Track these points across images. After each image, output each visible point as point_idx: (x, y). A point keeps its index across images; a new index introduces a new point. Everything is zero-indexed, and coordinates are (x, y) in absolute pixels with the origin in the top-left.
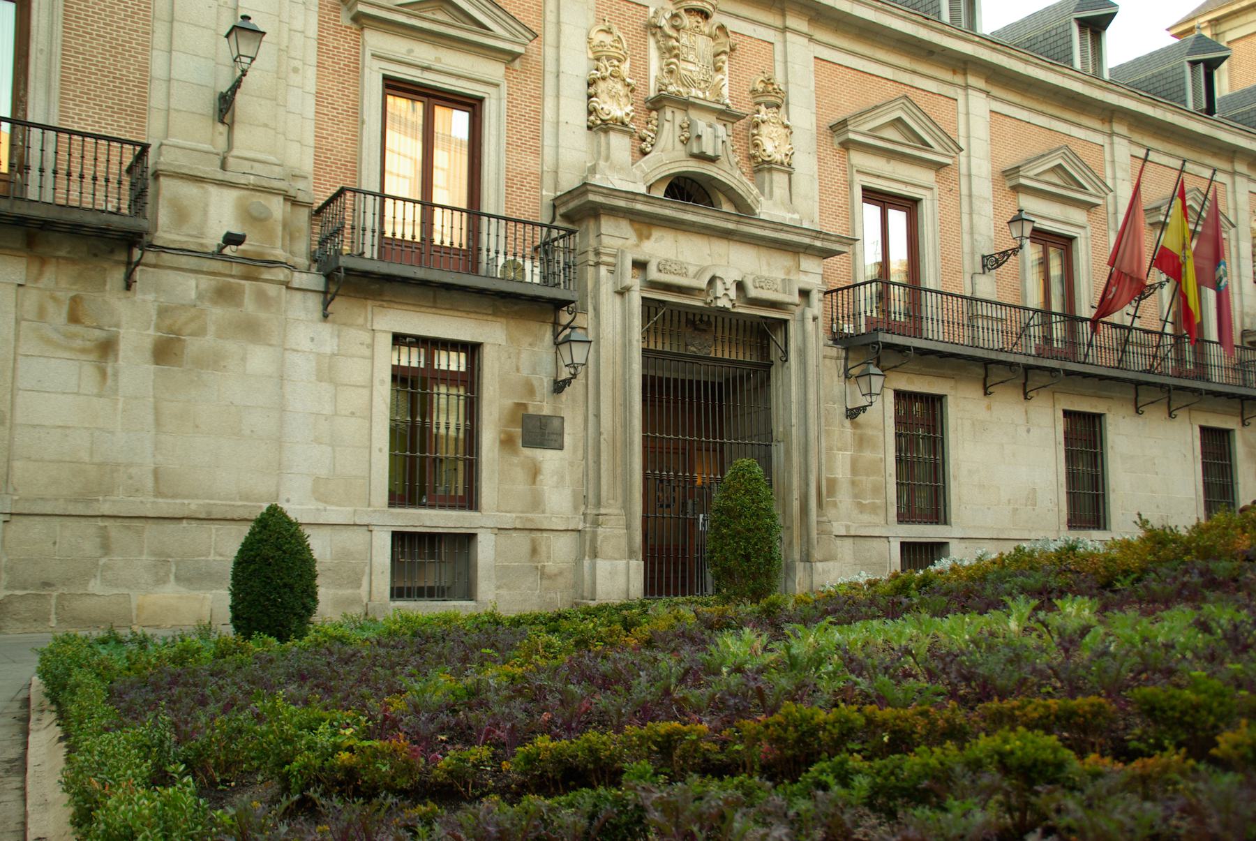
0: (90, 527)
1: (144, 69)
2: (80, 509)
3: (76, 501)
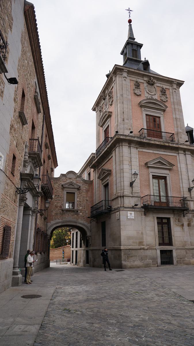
0: (184, 251)
1: (179, 186)
2: (183, 248)
3: (183, 247)
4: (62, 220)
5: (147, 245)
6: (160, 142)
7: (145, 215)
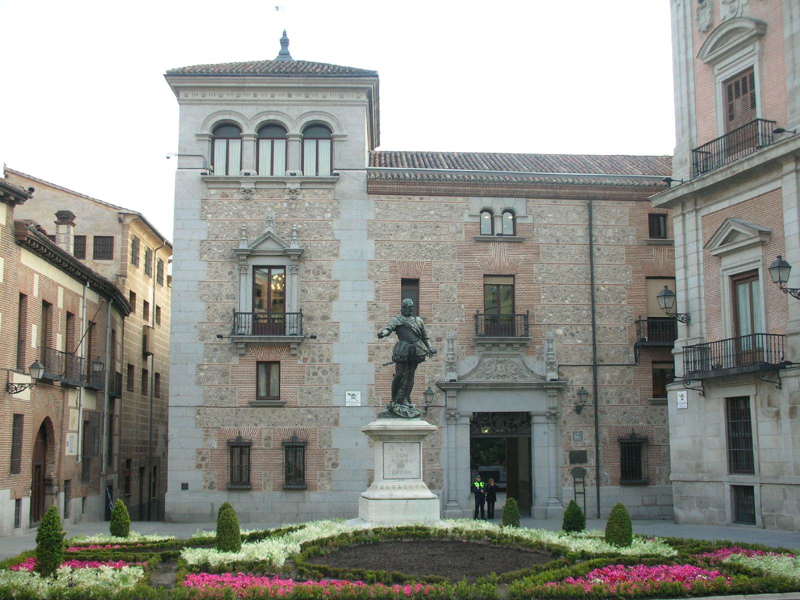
5: (709, 472)
6: (724, 173)
7: (704, 395)
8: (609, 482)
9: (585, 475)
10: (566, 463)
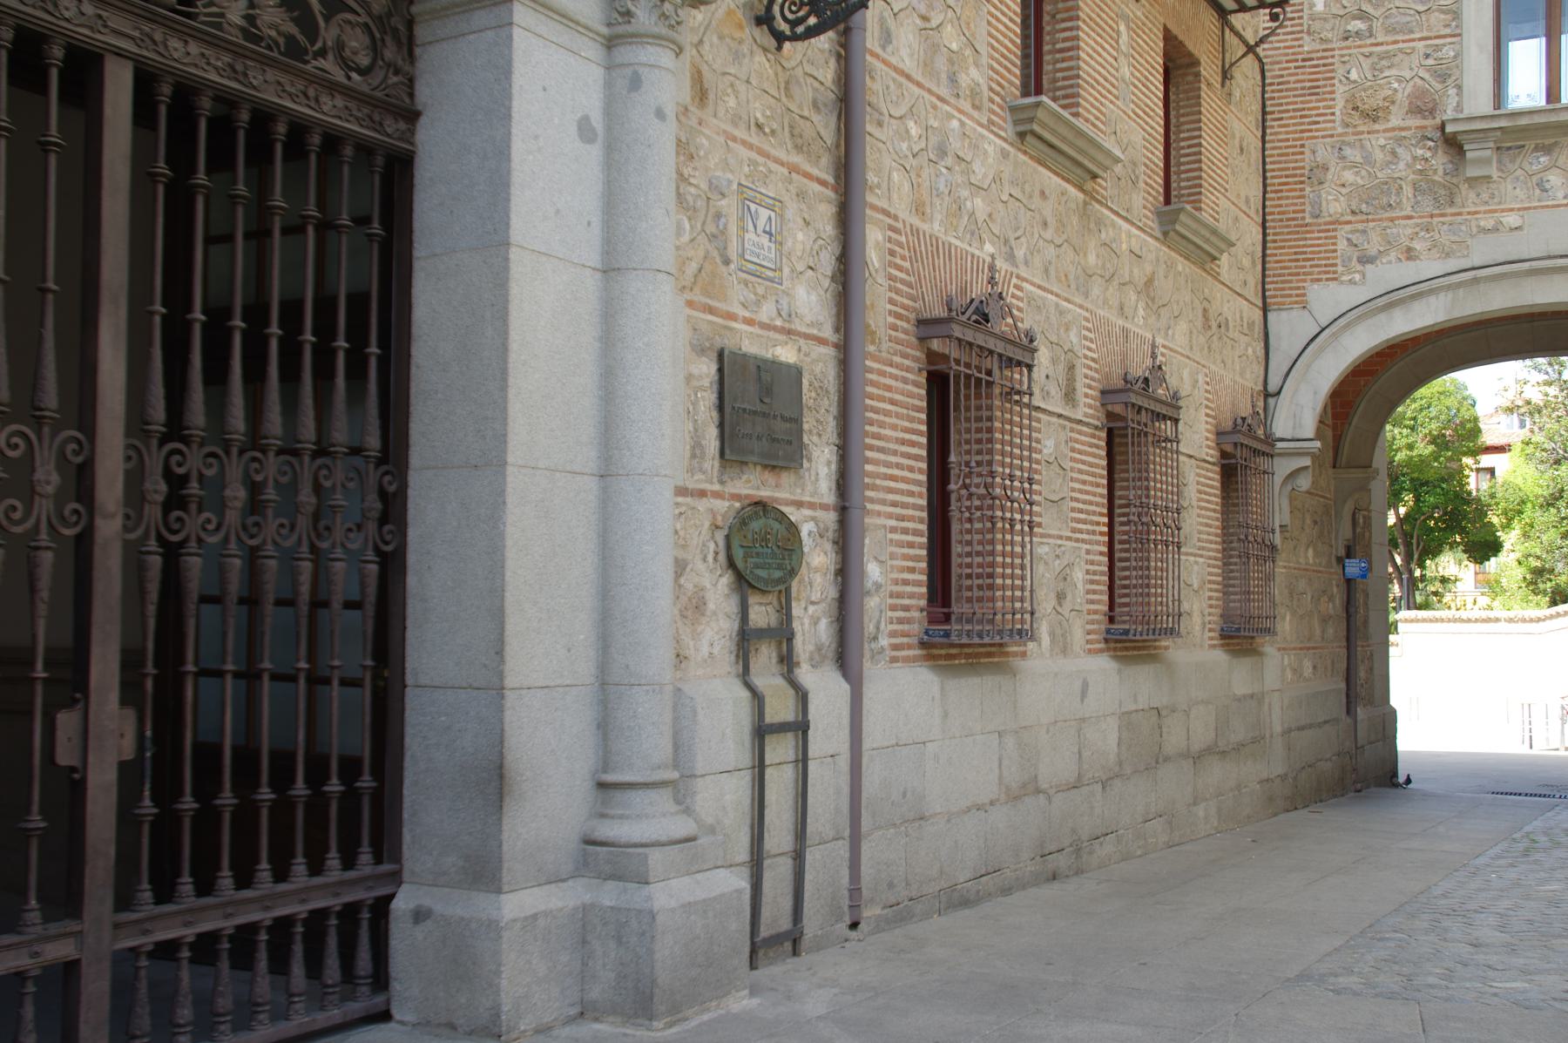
4: (1453, 264)
8: (884, 642)
9: (793, 573)
10: (697, 450)
